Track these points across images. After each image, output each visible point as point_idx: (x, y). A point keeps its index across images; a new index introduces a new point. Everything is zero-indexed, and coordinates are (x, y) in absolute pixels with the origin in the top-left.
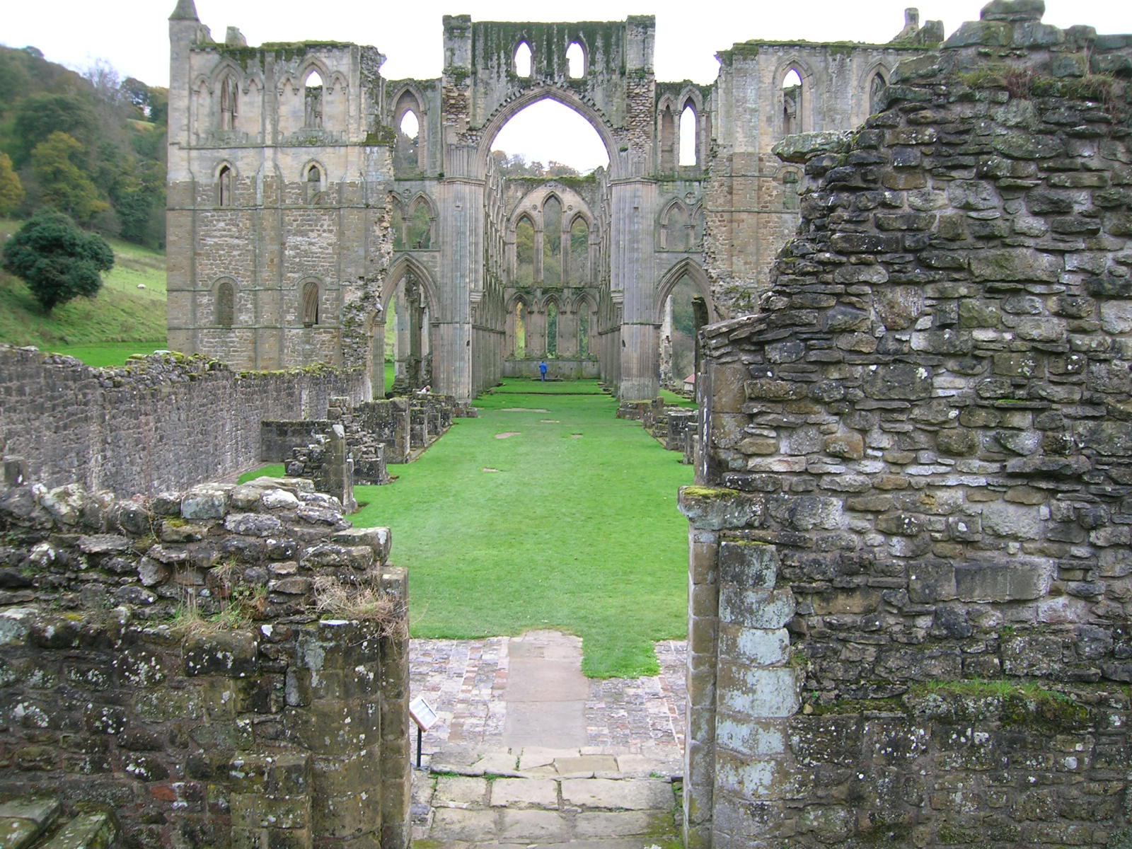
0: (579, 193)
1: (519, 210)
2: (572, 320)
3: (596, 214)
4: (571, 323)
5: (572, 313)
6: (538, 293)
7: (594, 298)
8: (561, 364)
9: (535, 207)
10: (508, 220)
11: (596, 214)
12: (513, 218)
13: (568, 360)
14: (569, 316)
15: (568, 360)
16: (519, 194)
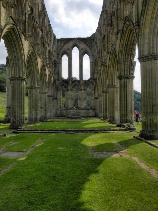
0: (86, 43)
1: (62, 50)
2: (84, 93)
3: (93, 51)
4: (84, 94)
5: (84, 90)
6: (70, 82)
7: (93, 84)
8: (80, 111)
9: (68, 49)
10: (58, 54)
11: (93, 51)
12: (60, 53)
13: (83, 109)
14: (83, 91)
15: (83, 109)
16: (62, 44)
